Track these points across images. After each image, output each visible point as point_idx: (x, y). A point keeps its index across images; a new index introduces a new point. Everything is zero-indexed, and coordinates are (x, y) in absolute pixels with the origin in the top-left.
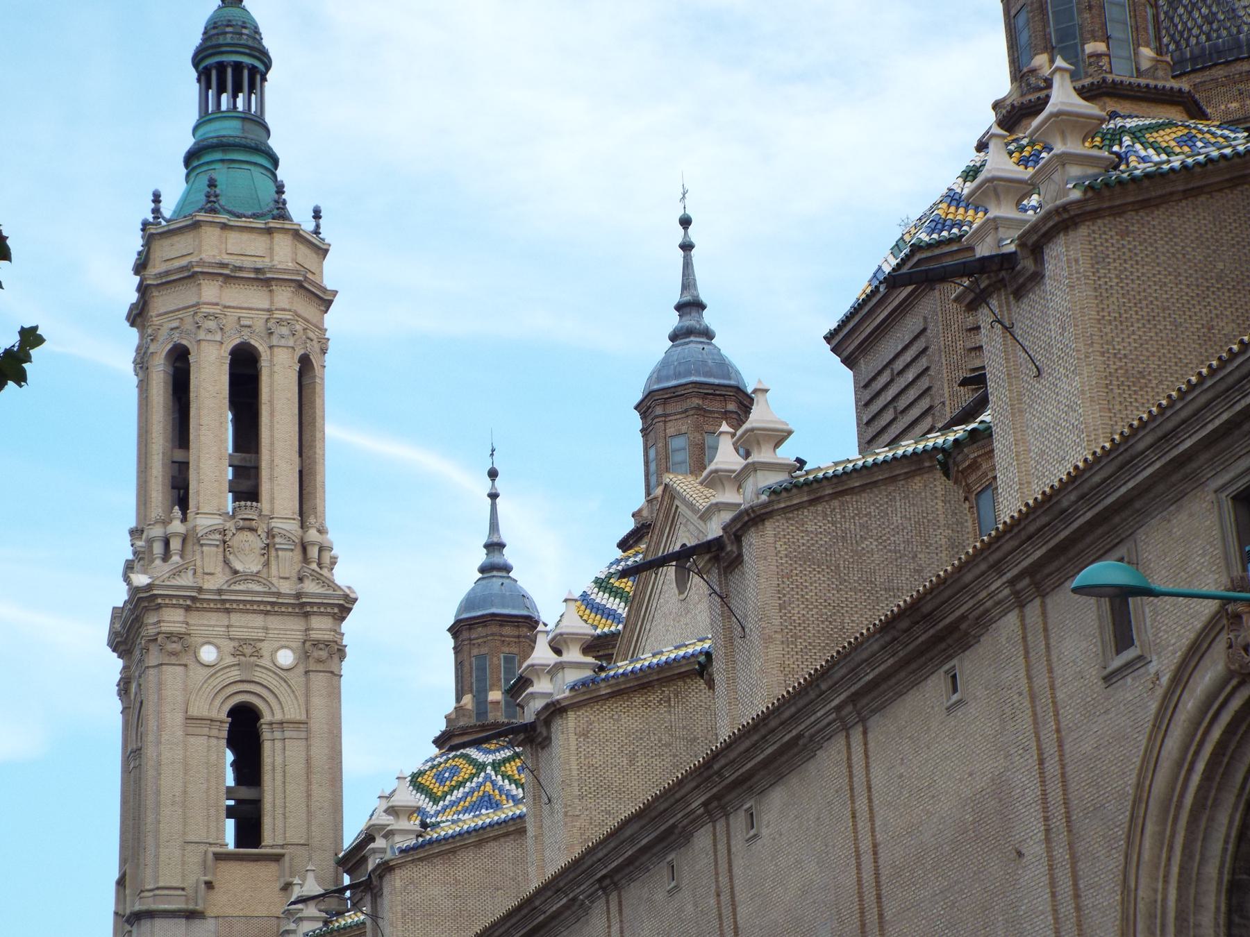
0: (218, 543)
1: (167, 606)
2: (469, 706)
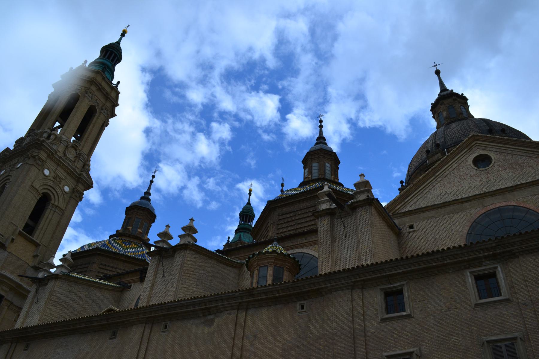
0: (66, 145)
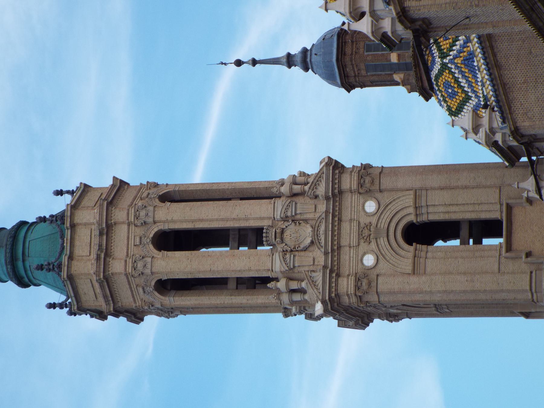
0: (292, 256)
1: (336, 290)
2: (402, 76)
